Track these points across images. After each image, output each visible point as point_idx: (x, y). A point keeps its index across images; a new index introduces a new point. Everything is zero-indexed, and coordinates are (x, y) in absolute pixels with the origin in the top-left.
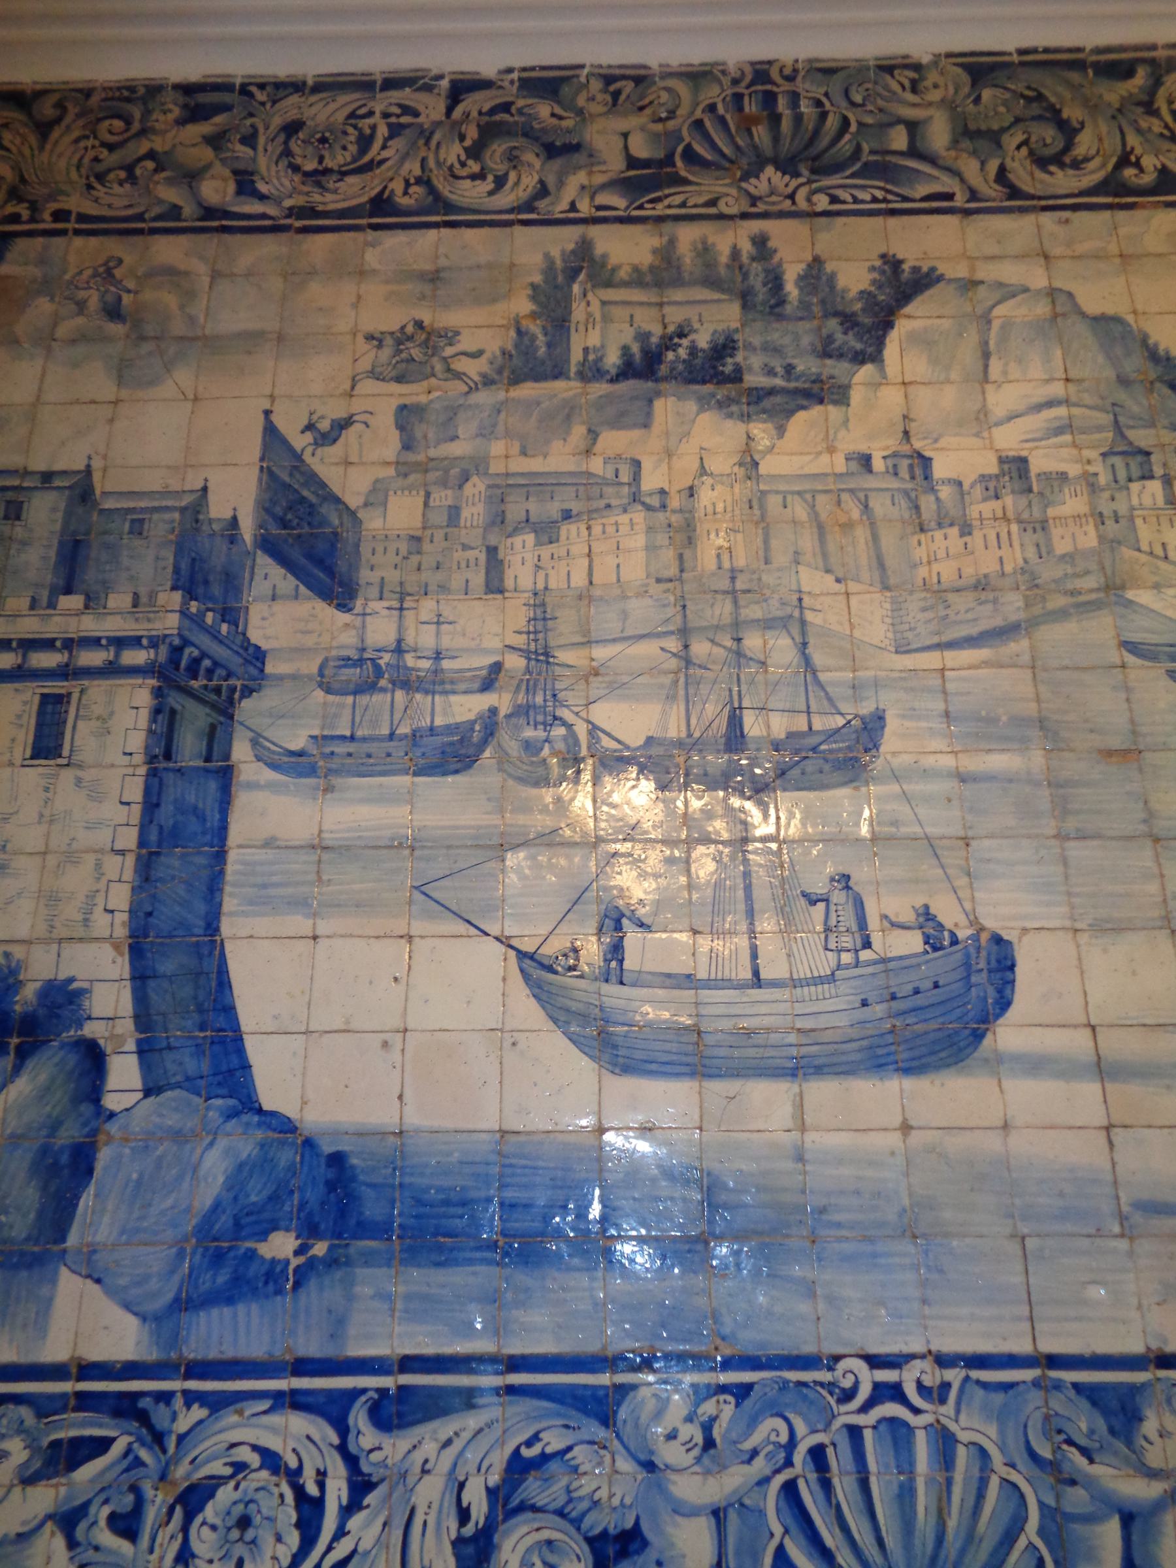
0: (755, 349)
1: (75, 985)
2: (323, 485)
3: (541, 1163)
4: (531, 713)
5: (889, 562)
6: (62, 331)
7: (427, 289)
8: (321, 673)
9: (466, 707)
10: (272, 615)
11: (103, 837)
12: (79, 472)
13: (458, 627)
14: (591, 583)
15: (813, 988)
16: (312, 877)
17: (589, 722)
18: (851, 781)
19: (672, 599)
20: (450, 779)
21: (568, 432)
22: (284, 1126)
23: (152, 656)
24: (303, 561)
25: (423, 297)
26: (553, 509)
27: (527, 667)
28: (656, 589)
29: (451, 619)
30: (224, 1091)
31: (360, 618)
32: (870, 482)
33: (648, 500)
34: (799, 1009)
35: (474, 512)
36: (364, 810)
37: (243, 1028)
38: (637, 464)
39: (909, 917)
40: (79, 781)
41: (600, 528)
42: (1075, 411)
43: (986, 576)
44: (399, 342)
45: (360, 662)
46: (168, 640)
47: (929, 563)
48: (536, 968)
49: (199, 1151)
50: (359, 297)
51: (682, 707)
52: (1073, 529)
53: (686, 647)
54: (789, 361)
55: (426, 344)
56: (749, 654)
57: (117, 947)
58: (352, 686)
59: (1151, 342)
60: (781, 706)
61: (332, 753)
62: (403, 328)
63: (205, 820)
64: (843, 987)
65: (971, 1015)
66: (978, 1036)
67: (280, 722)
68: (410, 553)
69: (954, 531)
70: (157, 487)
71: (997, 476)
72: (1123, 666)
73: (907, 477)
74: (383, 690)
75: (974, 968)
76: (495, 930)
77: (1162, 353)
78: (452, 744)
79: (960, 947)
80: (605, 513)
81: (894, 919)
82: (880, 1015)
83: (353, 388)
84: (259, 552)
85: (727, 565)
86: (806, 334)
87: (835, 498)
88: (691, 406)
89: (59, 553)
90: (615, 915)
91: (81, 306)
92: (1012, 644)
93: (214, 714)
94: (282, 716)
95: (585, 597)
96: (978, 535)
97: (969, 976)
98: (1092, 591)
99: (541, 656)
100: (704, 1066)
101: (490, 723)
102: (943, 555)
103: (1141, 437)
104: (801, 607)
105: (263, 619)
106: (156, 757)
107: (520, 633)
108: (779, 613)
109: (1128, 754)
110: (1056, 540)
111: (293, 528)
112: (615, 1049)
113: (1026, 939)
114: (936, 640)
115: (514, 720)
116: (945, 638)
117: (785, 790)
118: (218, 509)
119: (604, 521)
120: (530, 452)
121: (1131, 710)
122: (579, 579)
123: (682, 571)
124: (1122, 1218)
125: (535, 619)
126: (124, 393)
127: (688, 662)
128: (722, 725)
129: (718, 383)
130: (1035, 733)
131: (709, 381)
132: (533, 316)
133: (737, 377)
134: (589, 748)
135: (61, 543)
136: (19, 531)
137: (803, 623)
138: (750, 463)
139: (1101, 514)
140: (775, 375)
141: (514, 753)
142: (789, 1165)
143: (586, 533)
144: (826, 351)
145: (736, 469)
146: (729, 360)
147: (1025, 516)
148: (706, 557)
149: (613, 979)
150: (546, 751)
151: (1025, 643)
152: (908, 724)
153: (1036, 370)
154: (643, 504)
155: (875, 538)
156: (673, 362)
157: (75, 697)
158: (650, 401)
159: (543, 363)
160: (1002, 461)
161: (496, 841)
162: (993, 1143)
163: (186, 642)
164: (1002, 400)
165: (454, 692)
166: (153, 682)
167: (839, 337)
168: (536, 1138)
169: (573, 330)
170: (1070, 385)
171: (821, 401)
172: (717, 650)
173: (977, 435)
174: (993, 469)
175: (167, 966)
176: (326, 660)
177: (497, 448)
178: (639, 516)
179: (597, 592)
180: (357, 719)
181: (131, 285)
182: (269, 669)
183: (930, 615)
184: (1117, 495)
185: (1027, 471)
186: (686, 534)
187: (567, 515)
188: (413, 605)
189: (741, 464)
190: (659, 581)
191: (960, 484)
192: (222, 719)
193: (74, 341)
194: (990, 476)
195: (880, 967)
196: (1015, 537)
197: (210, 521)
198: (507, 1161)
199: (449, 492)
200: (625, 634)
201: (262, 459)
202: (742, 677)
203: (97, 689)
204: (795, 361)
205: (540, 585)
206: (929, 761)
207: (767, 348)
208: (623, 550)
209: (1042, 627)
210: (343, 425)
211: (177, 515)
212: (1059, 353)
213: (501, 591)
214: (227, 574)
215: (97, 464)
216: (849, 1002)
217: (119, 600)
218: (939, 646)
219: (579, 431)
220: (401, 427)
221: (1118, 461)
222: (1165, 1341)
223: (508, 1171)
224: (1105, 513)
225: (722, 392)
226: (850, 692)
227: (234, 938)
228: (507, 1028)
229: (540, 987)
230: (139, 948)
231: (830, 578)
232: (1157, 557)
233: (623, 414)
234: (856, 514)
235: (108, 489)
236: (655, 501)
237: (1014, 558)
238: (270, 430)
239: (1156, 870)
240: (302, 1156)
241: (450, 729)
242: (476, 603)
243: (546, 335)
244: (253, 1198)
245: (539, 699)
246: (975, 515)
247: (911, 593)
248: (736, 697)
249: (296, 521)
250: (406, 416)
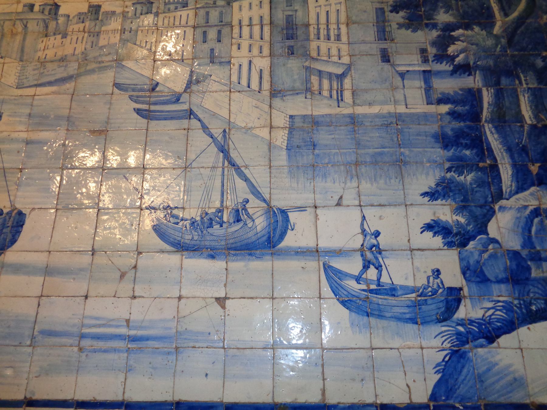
5: (26, 50)
32: (31, 16)
43: (66, 56)
47: (44, 50)
96: (69, 38)
113: (33, 213)
114: (36, 82)
116: (39, 82)
121: (109, 113)
124: (33, 337)
147: (92, 30)
151: (73, 84)
152: (11, 119)
155: (24, 40)
160: (90, 6)
174: (86, 10)
183: (36, 72)
185: (99, 11)
191: (69, 16)
194: (83, 13)
196: (85, 39)
206: (15, 135)
209: (83, 77)
218: (36, 86)
222: (34, 394)
224: (127, 29)
237: (80, 48)
246: (71, 30)
247: (31, 63)
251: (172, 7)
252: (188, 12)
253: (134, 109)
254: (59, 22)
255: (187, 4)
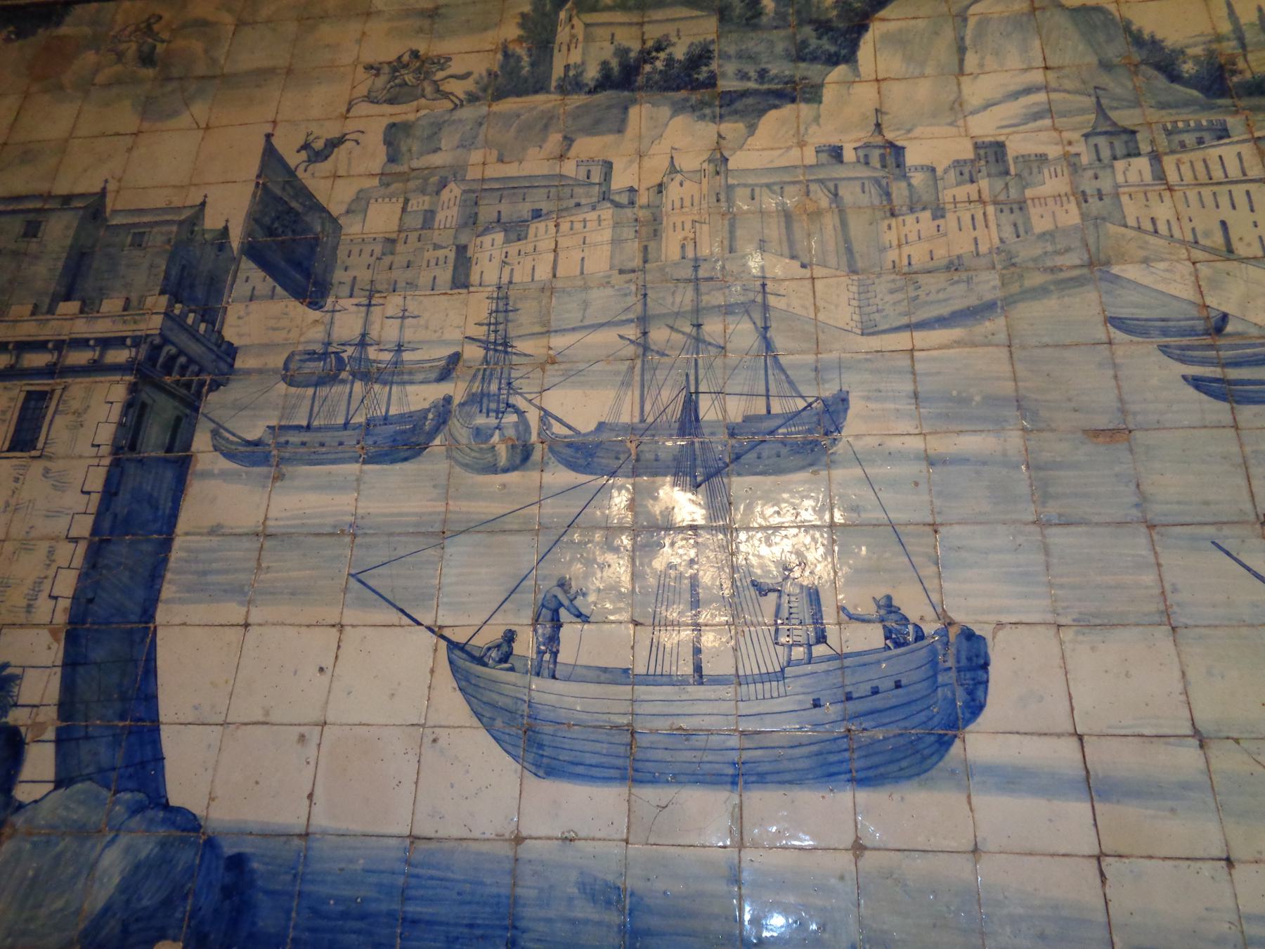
0: (729, 57)
1: (8, 671)
2: (311, 196)
3: (450, 875)
4: (485, 400)
5: (857, 247)
6: (100, 78)
7: (426, 23)
8: (286, 367)
9: (421, 397)
10: (248, 314)
11: (59, 526)
12: (95, 194)
13: (422, 321)
14: (554, 276)
15: (759, 686)
16: (254, 564)
17: (542, 409)
18: (811, 465)
19: (633, 288)
20: (398, 466)
21: (544, 140)
22: (186, 822)
23: (133, 354)
24: (283, 264)
25: (421, 30)
26: (525, 209)
27: (485, 357)
28: (618, 280)
29: (416, 313)
30: (130, 785)
31: (329, 315)
32: (839, 172)
33: (617, 198)
34: (744, 708)
35: (448, 214)
36: (313, 497)
37: (162, 718)
38: (608, 165)
39: (868, 609)
40: (47, 471)
41: (569, 225)
42: (1053, 96)
43: (959, 257)
44: (395, 70)
45: (324, 356)
46: (149, 340)
47: (899, 246)
48: (464, 660)
49: (99, 848)
50: (364, 34)
51: (637, 393)
52: (1053, 207)
53: (645, 334)
54: (763, 66)
55: (419, 70)
56: (707, 338)
57: (54, 633)
58: (315, 378)
59: (1134, 28)
60: (738, 390)
61: (287, 442)
62: (400, 58)
63: (157, 508)
64: (793, 686)
65: (936, 720)
66: (944, 744)
67: (243, 413)
68: (383, 254)
69: (927, 215)
70: (161, 204)
71: (972, 161)
72: (1110, 343)
73: (878, 165)
74: (343, 382)
75: (942, 666)
76: (427, 619)
77: (1146, 37)
78: (404, 432)
79: (925, 642)
80: (574, 211)
81: (852, 611)
82: (833, 717)
83: (348, 111)
84: (244, 258)
85: (690, 254)
86: (781, 41)
87: (804, 189)
88: (665, 111)
89: (66, 266)
90: (553, 605)
91: (120, 56)
92: (987, 323)
93: (182, 407)
94: (245, 410)
95: (548, 289)
97: (935, 676)
98: (1075, 267)
99: (498, 346)
100: (636, 770)
101: (444, 411)
102: (915, 239)
103: (1125, 117)
104: (764, 292)
105: (239, 318)
106: (122, 448)
107: (480, 324)
108: (742, 299)
109: (1116, 434)
110: (1035, 220)
111: (277, 236)
112: (538, 747)
113: (1001, 634)
114: (905, 320)
115: (467, 408)
116: (914, 320)
117: (739, 475)
118: (212, 222)
119: (572, 218)
120: (506, 160)
121: (1119, 387)
122: (543, 273)
123: (645, 261)
125: (497, 311)
126: (146, 125)
127: (646, 349)
128: (676, 410)
129: (693, 89)
130: (1012, 413)
131: (685, 88)
132: (520, 40)
133: (711, 82)
134: (539, 434)
135: (68, 258)
136: (33, 246)
137: (765, 307)
138: (719, 160)
139: (1083, 193)
140: (749, 79)
141: (464, 441)
142: (722, 887)
143: (554, 230)
144: (801, 54)
145: (705, 165)
146: (704, 69)
147: (1002, 197)
148: (670, 247)
149: (546, 673)
150: (496, 438)
151: (1001, 321)
152: (872, 405)
153: (1014, 59)
154: (612, 201)
155: (844, 224)
156: (649, 73)
157: (58, 393)
158: (626, 109)
159: (526, 80)
160: (977, 146)
161: (437, 528)
162: (960, 868)
163: (166, 341)
164: (976, 90)
165: (412, 383)
166: (130, 378)
167: (813, 43)
168: (447, 845)
169: (556, 51)
170: (1048, 72)
171: (793, 100)
172: (676, 337)
173: (951, 124)
174: (970, 155)
175: (98, 654)
176: (293, 354)
177: (476, 156)
178: (607, 212)
179: (559, 284)
180: (316, 409)
181: (165, 35)
182: (238, 364)
183: (900, 296)
184: (1101, 174)
185: (1004, 154)
186: (653, 227)
187: (537, 214)
188: (381, 301)
189: (710, 161)
190: (621, 272)
191: (933, 170)
192: (188, 411)
193: (109, 85)
194: (965, 161)
195: (836, 664)
196: (991, 217)
197: (204, 232)
198: (416, 871)
199: (427, 198)
200: (586, 323)
201: (259, 176)
202: (700, 362)
203: (78, 387)
204: (769, 66)
205: (505, 279)
206: (895, 444)
207: (740, 56)
208: (589, 246)
209: (1021, 306)
210: (334, 144)
211: (175, 228)
212: (1037, 43)
213: (466, 286)
214: (212, 279)
215: (111, 187)
216: (800, 702)
217: (111, 305)
218: (909, 327)
219: (555, 139)
220: (389, 142)
221: (1102, 141)
223: (413, 881)
224: (1088, 192)
225: (695, 97)
226: (813, 374)
227: (168, 625)
228: (430, 723)
229: (468, 681)
230: (76, 635)
231: (796, 264)
232: (1146, 232)
233: (598, 122)
234: (824, 202)
235: (119, 207)
236: (624, 199)
237: (988, 239)
238: (270, 153)
239: (1152, 559)
240: (202, 857)
241: (402, 418)
242: (442, 297)
243: (530, 56)
244: (145, 902)
245: (494, 388)
247: (879, 275)
248: (692, 382)
249: (280, 230)
250: (394, 135)
251: (1189, 139)
252: (1238, 148)
253: (1185, 378)
254: (914, 182)
255: (1226, 130)
